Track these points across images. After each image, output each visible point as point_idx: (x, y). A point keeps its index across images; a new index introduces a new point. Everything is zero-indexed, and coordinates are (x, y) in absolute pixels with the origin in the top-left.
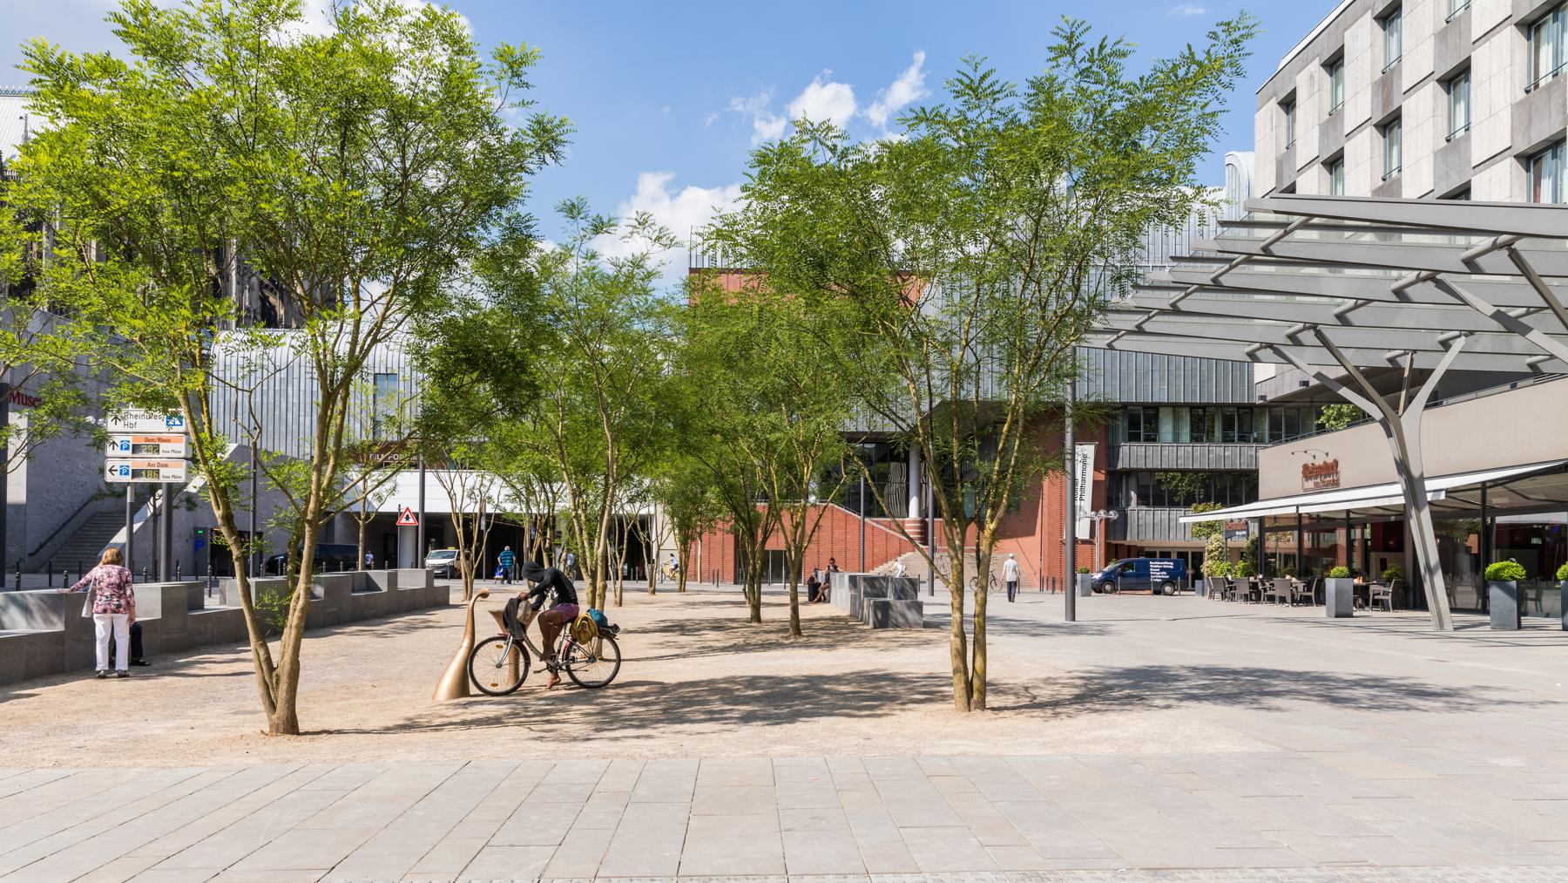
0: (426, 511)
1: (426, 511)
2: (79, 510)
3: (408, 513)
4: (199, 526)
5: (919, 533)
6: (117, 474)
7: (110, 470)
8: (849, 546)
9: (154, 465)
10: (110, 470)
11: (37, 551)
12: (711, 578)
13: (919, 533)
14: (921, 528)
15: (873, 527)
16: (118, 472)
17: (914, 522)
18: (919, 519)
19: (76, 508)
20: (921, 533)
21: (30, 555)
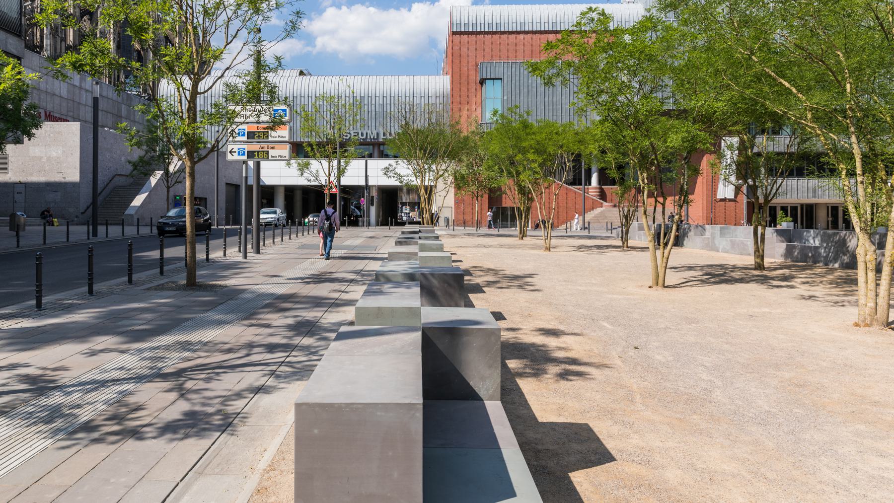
1: (341, 184)
2: (107, 185)
4: (176, 194)
5: (598, 196)
6: (236, 154)
7: (231, 152)
8: (560, 204)
9: (264, 148)
10: (231, 152)
11: (86, 211)
13: (598, 196)
14: (600, 192)
15: (575, 192)
16: (237, 153)
17: (595, 188)
18: (599, 186)
19: (106, 183)
20: (599, 196)
21: (82, 213)
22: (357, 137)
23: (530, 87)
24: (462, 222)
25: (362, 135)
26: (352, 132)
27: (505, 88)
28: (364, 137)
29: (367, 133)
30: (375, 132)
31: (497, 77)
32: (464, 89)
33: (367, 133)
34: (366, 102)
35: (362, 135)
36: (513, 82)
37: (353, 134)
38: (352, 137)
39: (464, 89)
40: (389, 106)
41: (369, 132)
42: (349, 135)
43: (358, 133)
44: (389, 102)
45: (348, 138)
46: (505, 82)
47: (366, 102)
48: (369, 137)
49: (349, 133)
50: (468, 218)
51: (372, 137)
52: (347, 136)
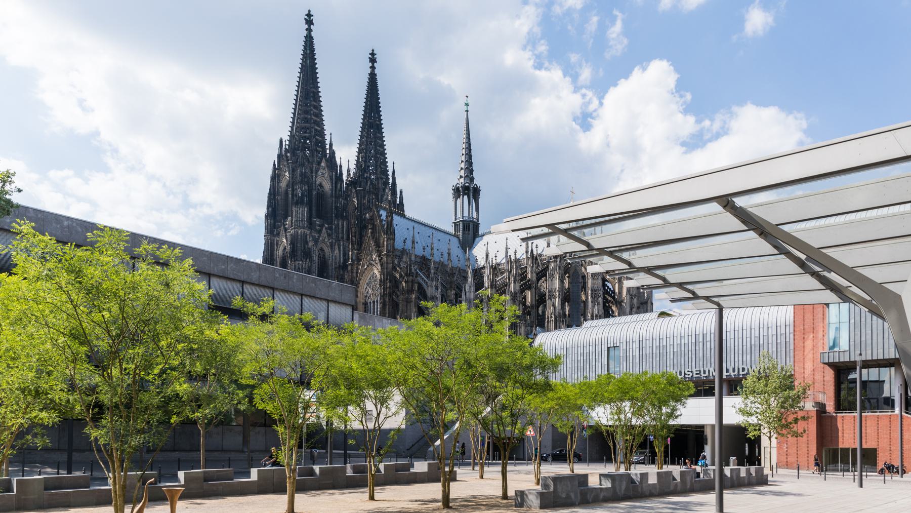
22: (699, 376)
25: (704, 372)
26: (694, 370)
29: (709, 371)
33: (709, 371)
34: (708, 339)
35: (704, 372)
37: (695, 373)
38: (695, 376)
40: (732, 341)
42: (691, 374)
43: (700, 371)
44: (732, 337)
45: (690, 376)
48: (711, 374)
49: (692, 372)
52: (689, 375)
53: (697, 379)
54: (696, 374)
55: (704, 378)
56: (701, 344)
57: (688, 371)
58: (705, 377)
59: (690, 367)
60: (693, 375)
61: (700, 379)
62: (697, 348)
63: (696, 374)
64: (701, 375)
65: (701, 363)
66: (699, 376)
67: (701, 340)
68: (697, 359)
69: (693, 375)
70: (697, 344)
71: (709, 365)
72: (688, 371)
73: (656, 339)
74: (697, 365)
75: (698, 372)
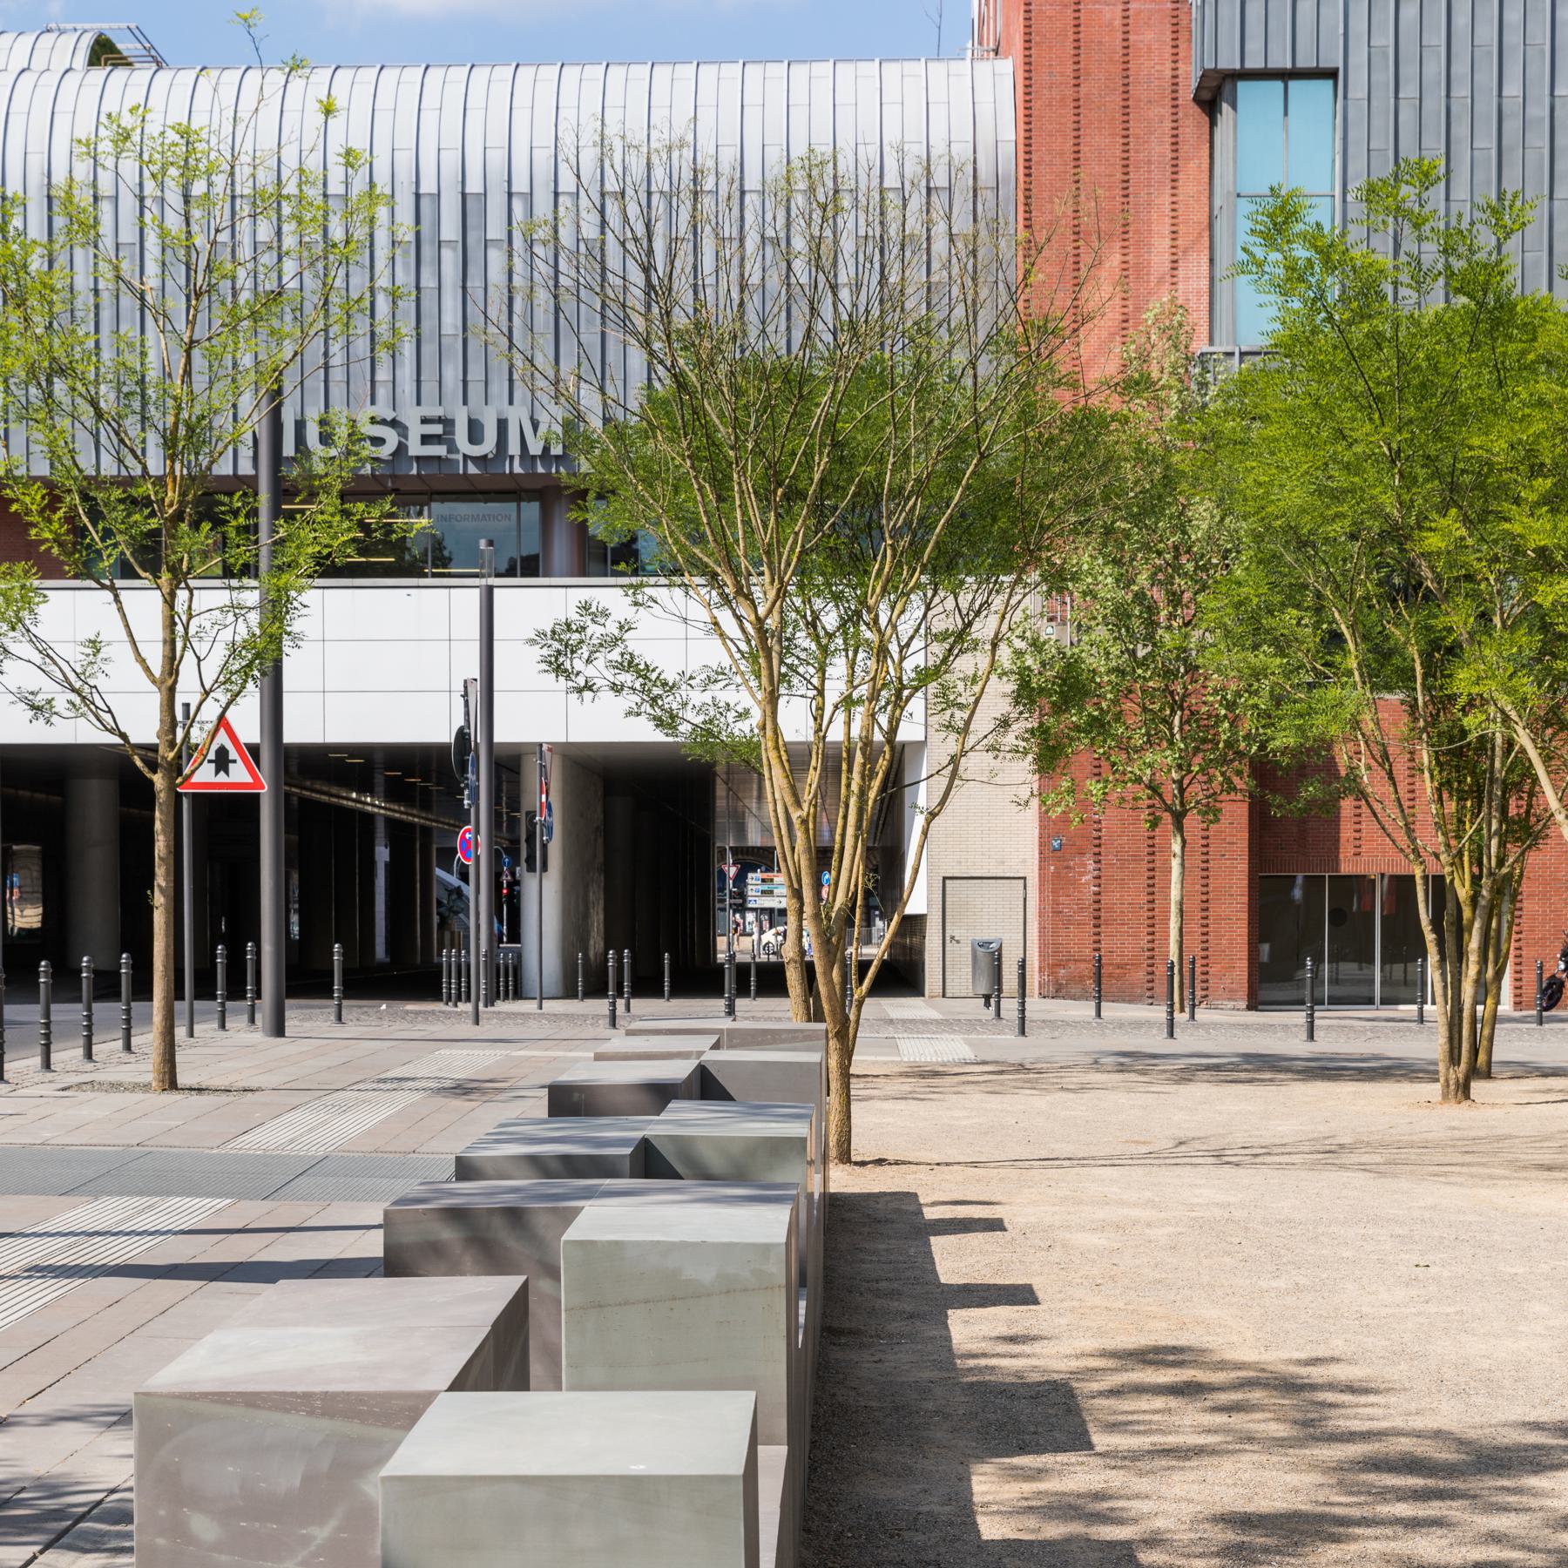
0: (497, 738)
3: (222, 738)
12: (1161, 988)
22: (440, 450)
23: (1512, 126)
24: (1087, 968)
26: (411, 416)
27: (1357, 133)
28: (488, 446)
29: (502, 425)
30: (552, 417)
31: (1306, 61)
32: (1101, 143)
33: (502, 425)
34: (496, 230)
36: (1409, 90)
37: (416, 431)
38: (415, 448)
39: (1101, 143)
41: (517, 416)
42: (392, 437)
43: (448, 423)
45: (385, 452)
46: (1358, 89)
47: (496, 230)
48: (514, 448)
49: (394, 423)
50: (1122, 944)
51: (535, 448)
52: (378, 441)
53: (432, 470)
54: (426, 439)
55: (472, 469)
56: (450, 259)
57: (373, 421)
58: (475, 460)
59: (383, 393)
60: (401, 449)
61: (446, 470)
62: (428, 281)
63: (426, 439)
64: (452, 448)
65: (452, 374)
66: (440, 450)
67: (450, 230)
68: (429, 349)
69: (401, 449)
70: (428, 251)
71: (499, 387)
72: (373, 421)
73: (116, 199)
74: (429, 387)
75: (437, 429)
